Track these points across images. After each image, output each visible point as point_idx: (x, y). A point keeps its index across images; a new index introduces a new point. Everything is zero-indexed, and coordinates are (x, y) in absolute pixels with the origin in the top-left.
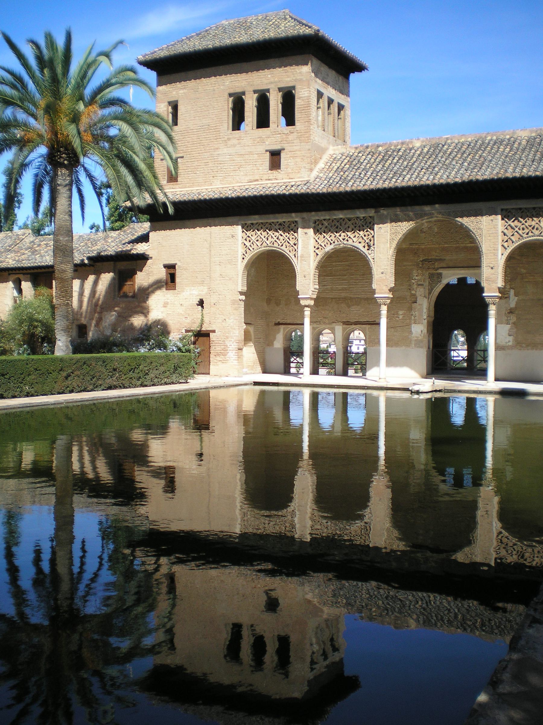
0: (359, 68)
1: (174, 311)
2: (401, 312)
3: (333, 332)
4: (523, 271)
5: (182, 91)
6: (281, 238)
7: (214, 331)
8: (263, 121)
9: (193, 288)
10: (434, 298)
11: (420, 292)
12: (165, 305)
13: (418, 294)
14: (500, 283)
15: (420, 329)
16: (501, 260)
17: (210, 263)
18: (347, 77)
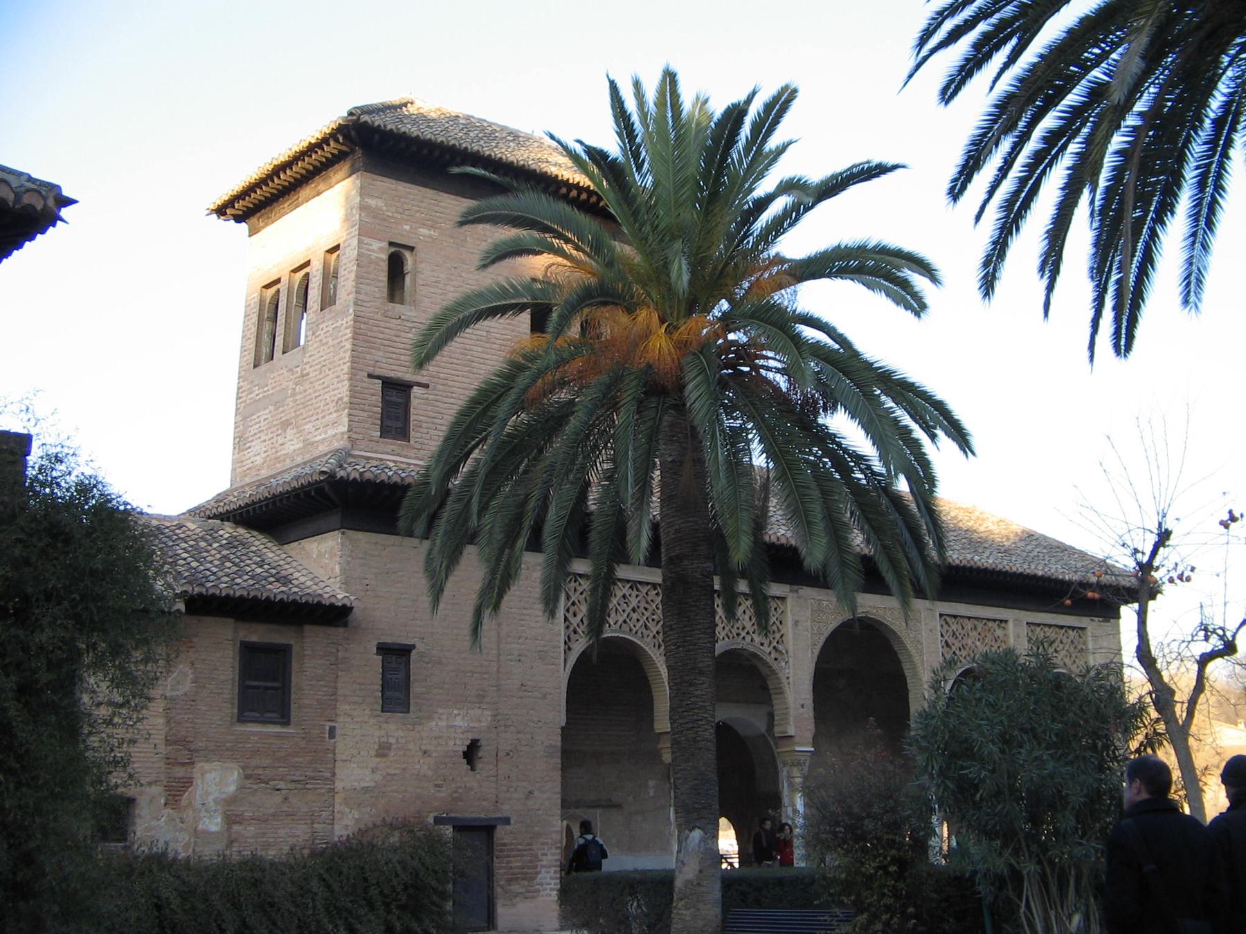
1: (404, 769)
2: (651, 783)
5: (424, 231)
6: (635, 616)
9: (456, 712)
12: (383, 750)
17: (499, 655)
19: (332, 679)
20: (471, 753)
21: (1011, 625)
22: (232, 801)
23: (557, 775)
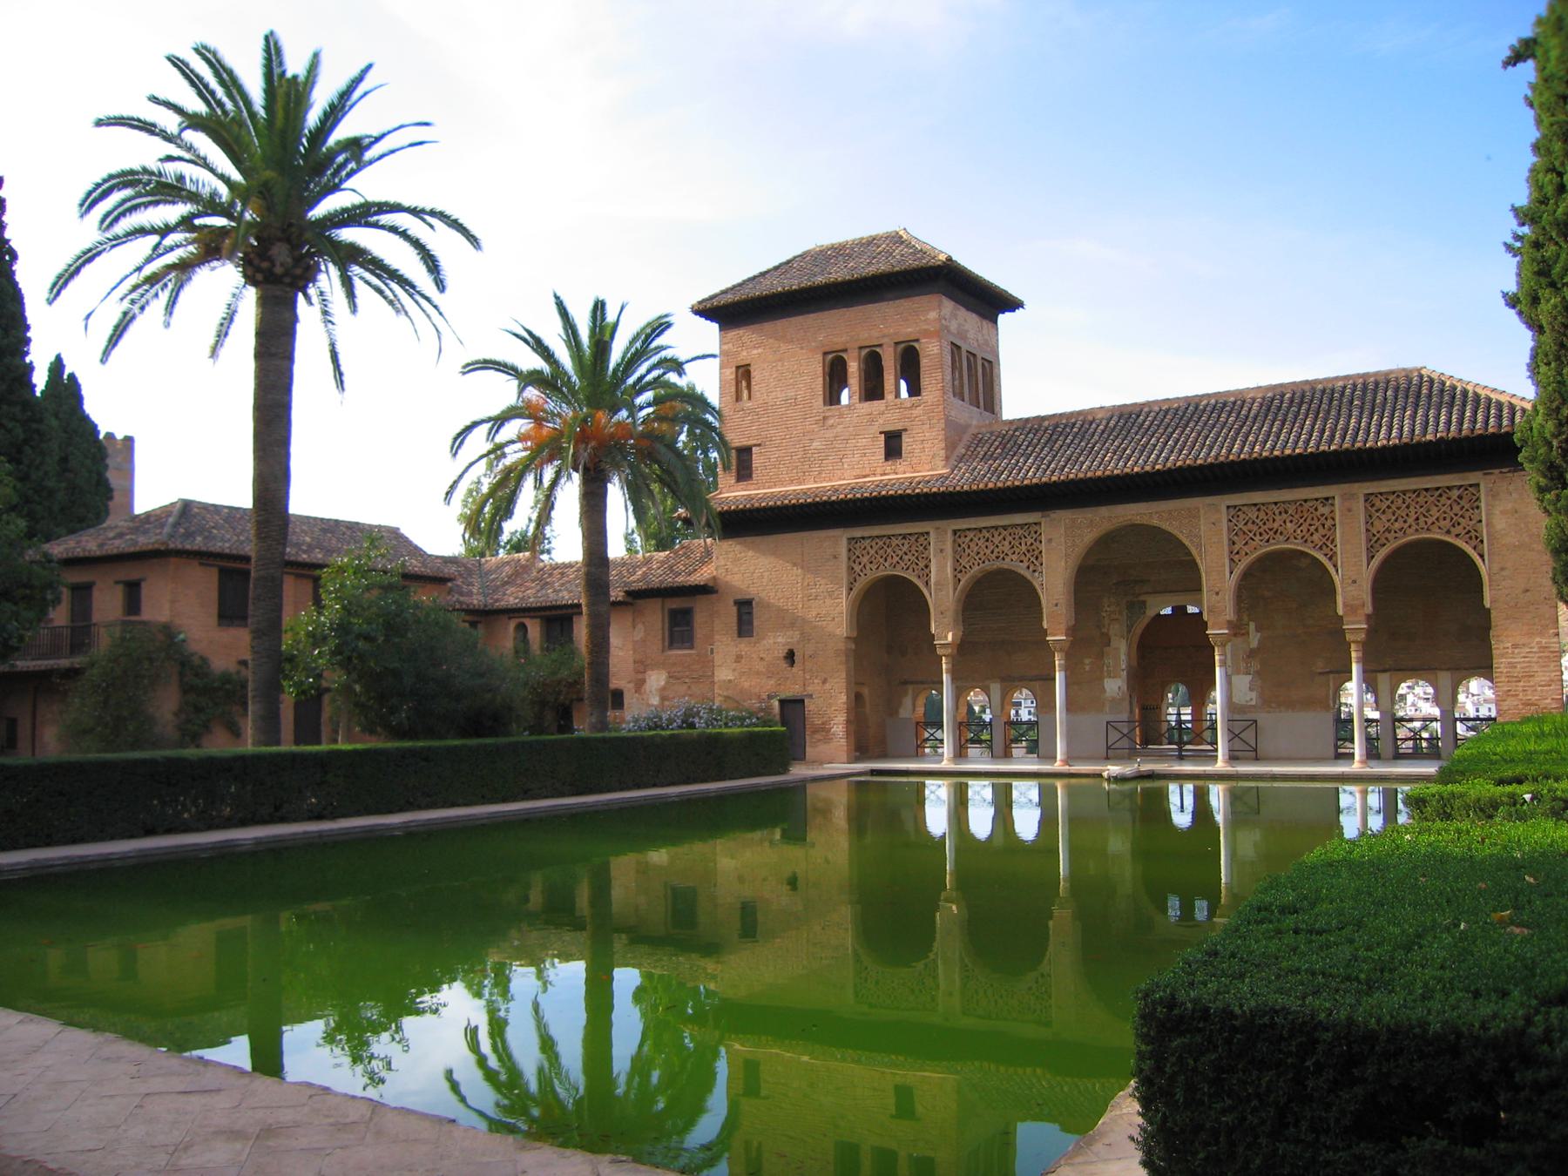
0: (1010, 304)
2: (1087, 661)
3: (986, 691)
4: (1267, 594)
7: (811, 696)
8: (873, 390)
10: (1136, 639)
11: (1115, 630)
12: (738, 658)
13: (1111, 632)
14: (1229, 614)
15: (1115, 686)
16: (1230, 582)
18: (995, 322)
19: (715, 625)
20: (790, 657)
21: (1337, 501)
22: (664, 689)
23: (843, 667)
